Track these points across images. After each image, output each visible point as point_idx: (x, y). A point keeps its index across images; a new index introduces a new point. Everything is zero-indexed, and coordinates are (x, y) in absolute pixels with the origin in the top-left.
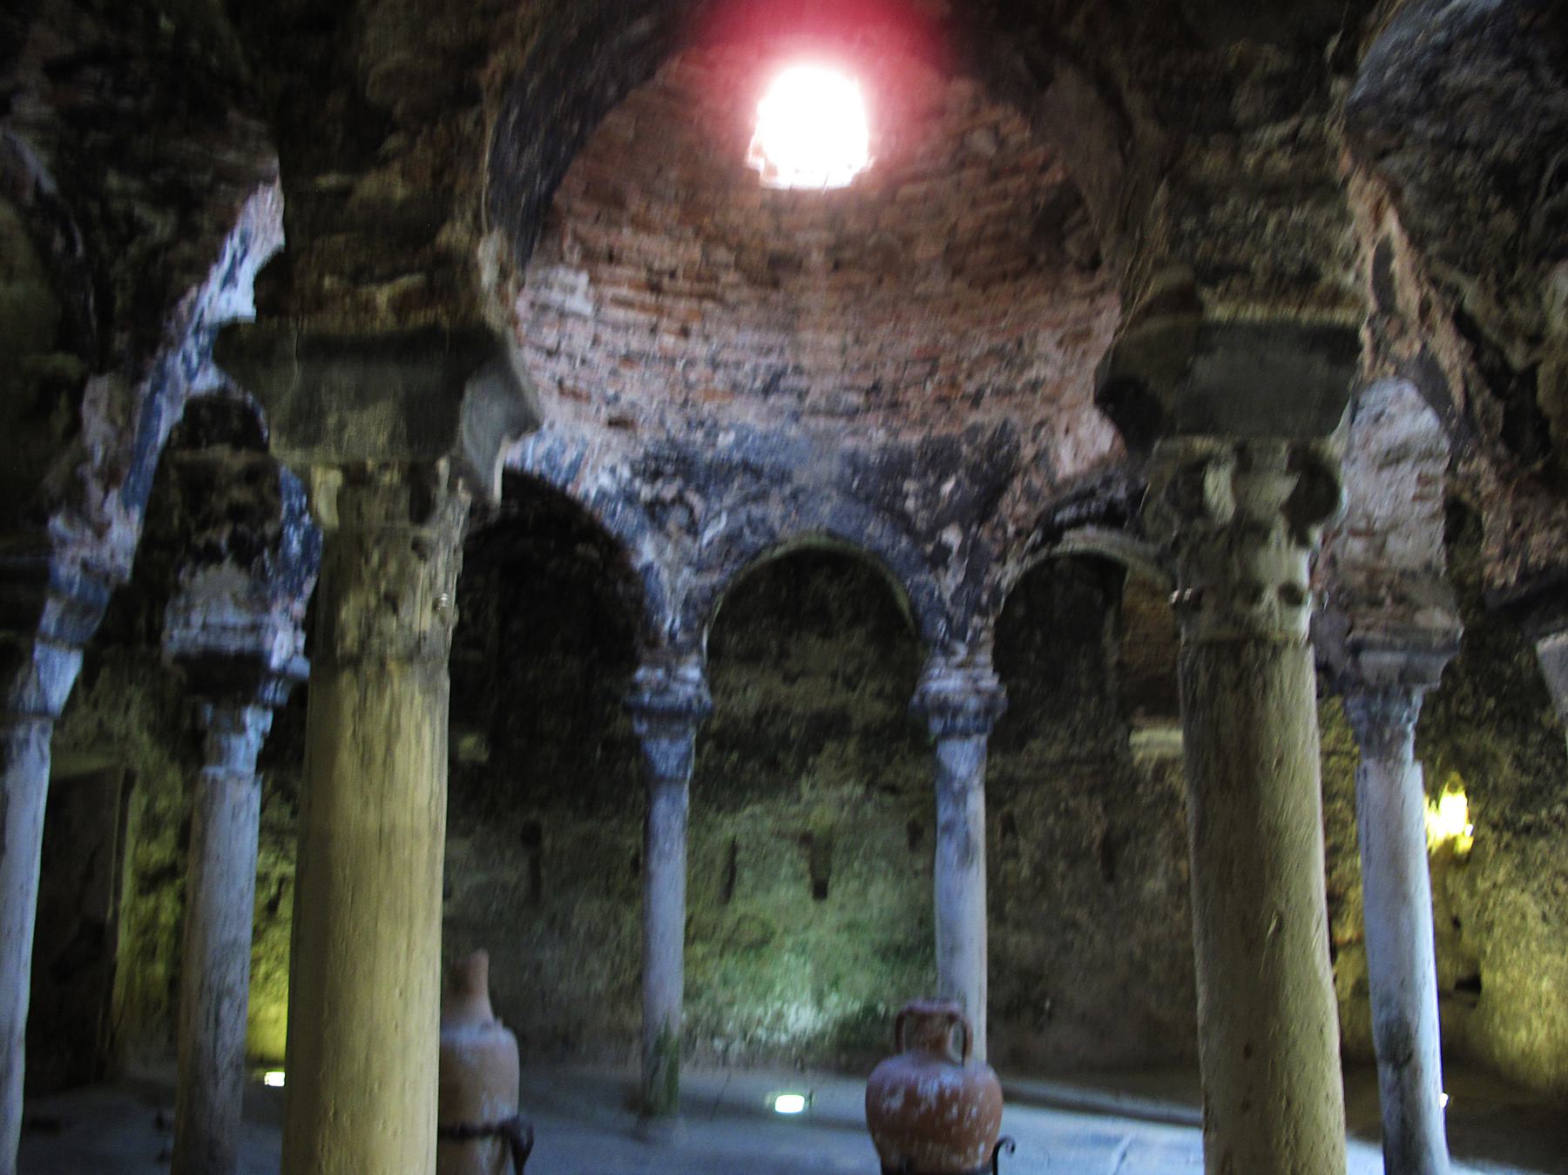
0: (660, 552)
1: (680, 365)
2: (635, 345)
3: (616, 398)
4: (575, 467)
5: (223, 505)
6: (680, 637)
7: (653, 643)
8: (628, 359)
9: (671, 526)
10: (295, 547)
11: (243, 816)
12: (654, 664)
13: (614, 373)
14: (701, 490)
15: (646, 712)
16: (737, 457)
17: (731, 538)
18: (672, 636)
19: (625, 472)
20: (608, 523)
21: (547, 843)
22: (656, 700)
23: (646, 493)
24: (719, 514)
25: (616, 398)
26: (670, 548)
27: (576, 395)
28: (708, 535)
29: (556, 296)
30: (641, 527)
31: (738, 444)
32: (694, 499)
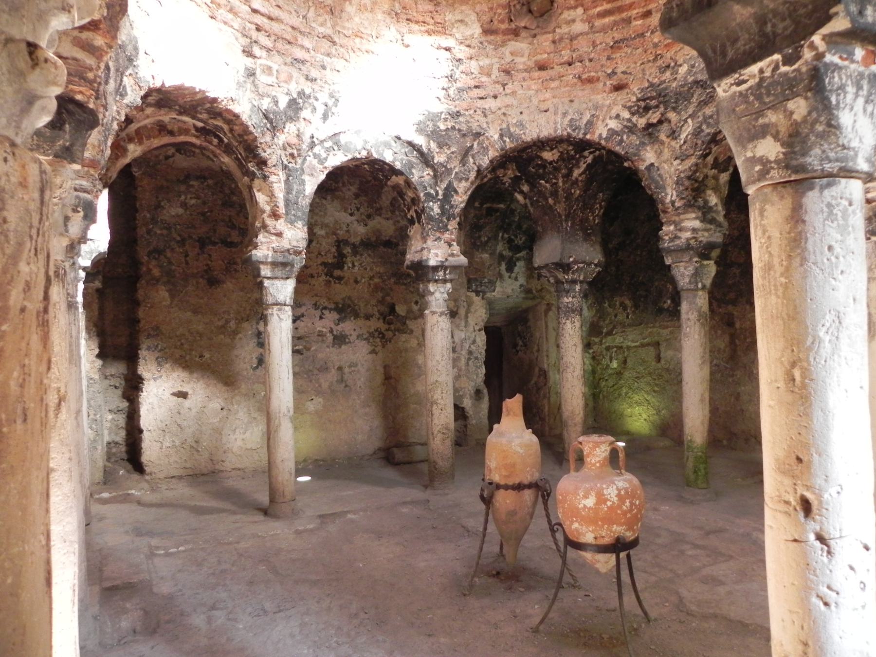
0: (659, 154)
1: (648, 34)
2: (618, 36)
3: (614, 73)
4: (590, 124)
5: (409, 200)
6: (677, 204)
7: (665, 212)
8: (616, 45)
9: (663, 137)
10: (436, 209)
11: (435, 330)
12: (670, 223)
13: (609, 58)
14: (674, 109)
15: (669, 251)
16: (691, 79)
17: (697, 132)
18: (673, 203)
19: (626, 115)
20: (617, 149)
21: (737, 325)
22: (670, 244)
23: (642, 122)
24: (686, 121)
25: (614, 73)
26: (666, 150)
27: (590, 81)
28: (683, 136)
29: (565, 29)
30: (643, 144)
31: (689, 72)
32: (672, 115)
